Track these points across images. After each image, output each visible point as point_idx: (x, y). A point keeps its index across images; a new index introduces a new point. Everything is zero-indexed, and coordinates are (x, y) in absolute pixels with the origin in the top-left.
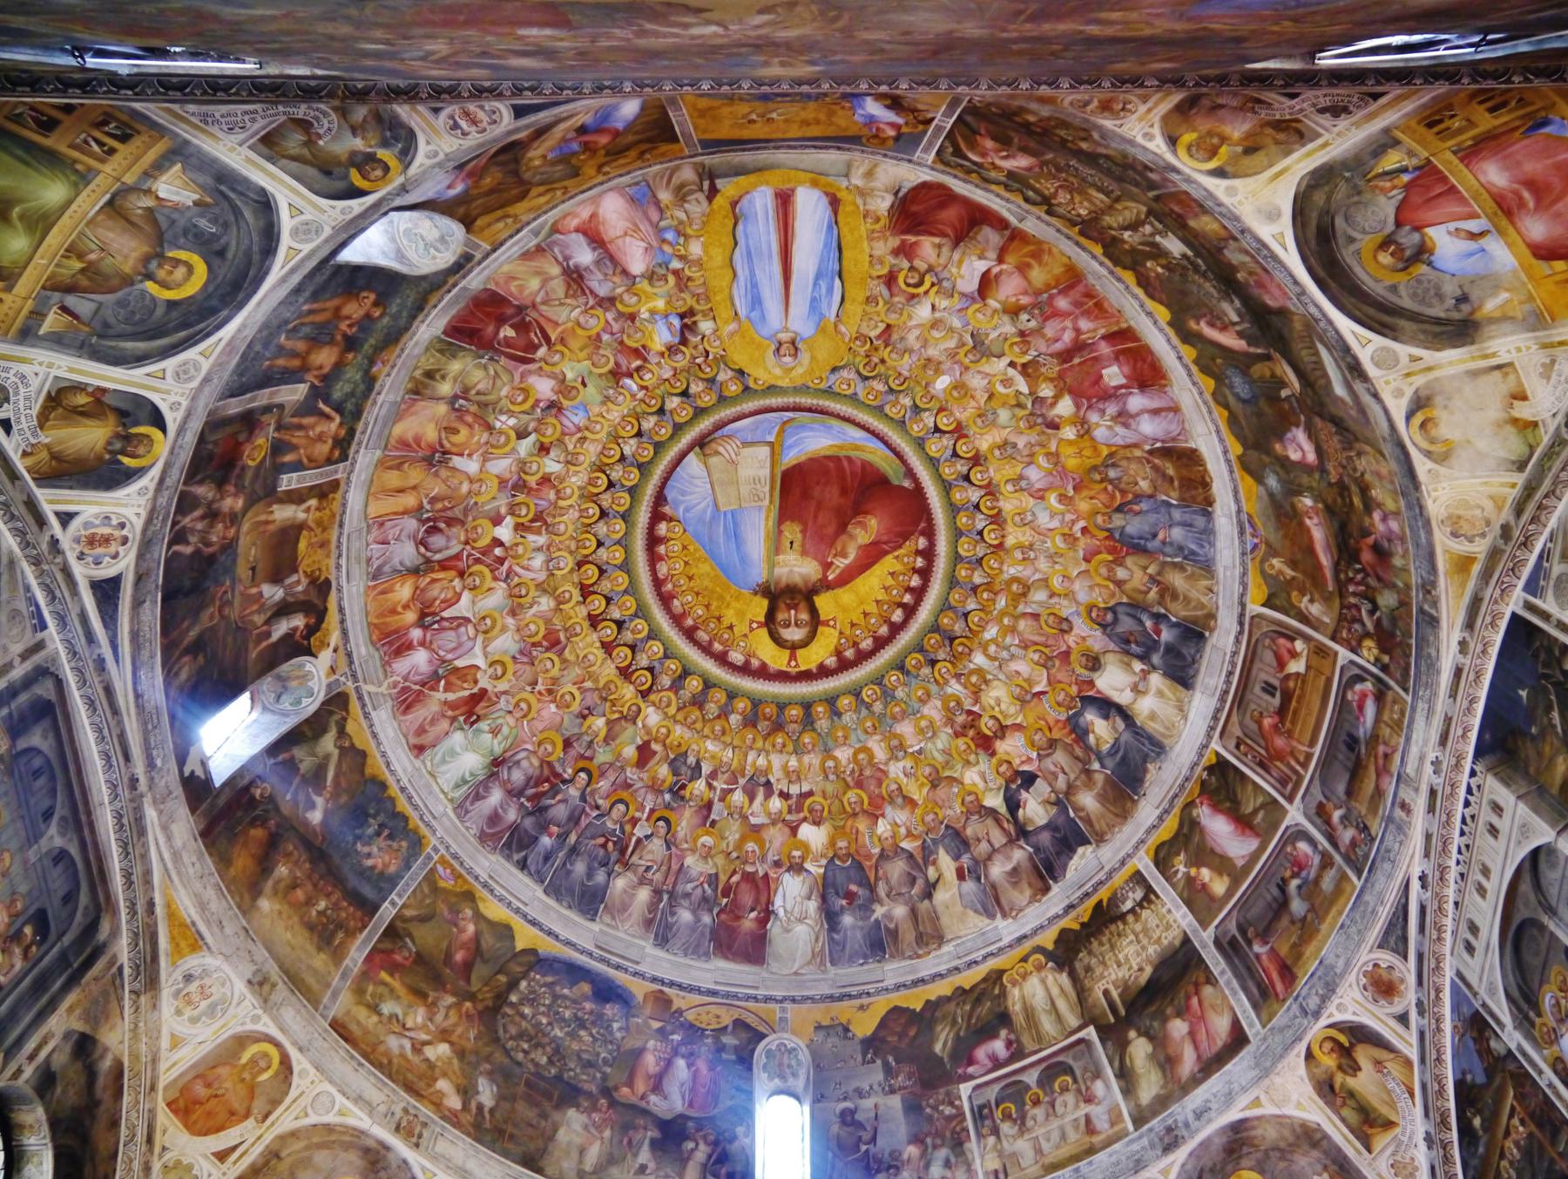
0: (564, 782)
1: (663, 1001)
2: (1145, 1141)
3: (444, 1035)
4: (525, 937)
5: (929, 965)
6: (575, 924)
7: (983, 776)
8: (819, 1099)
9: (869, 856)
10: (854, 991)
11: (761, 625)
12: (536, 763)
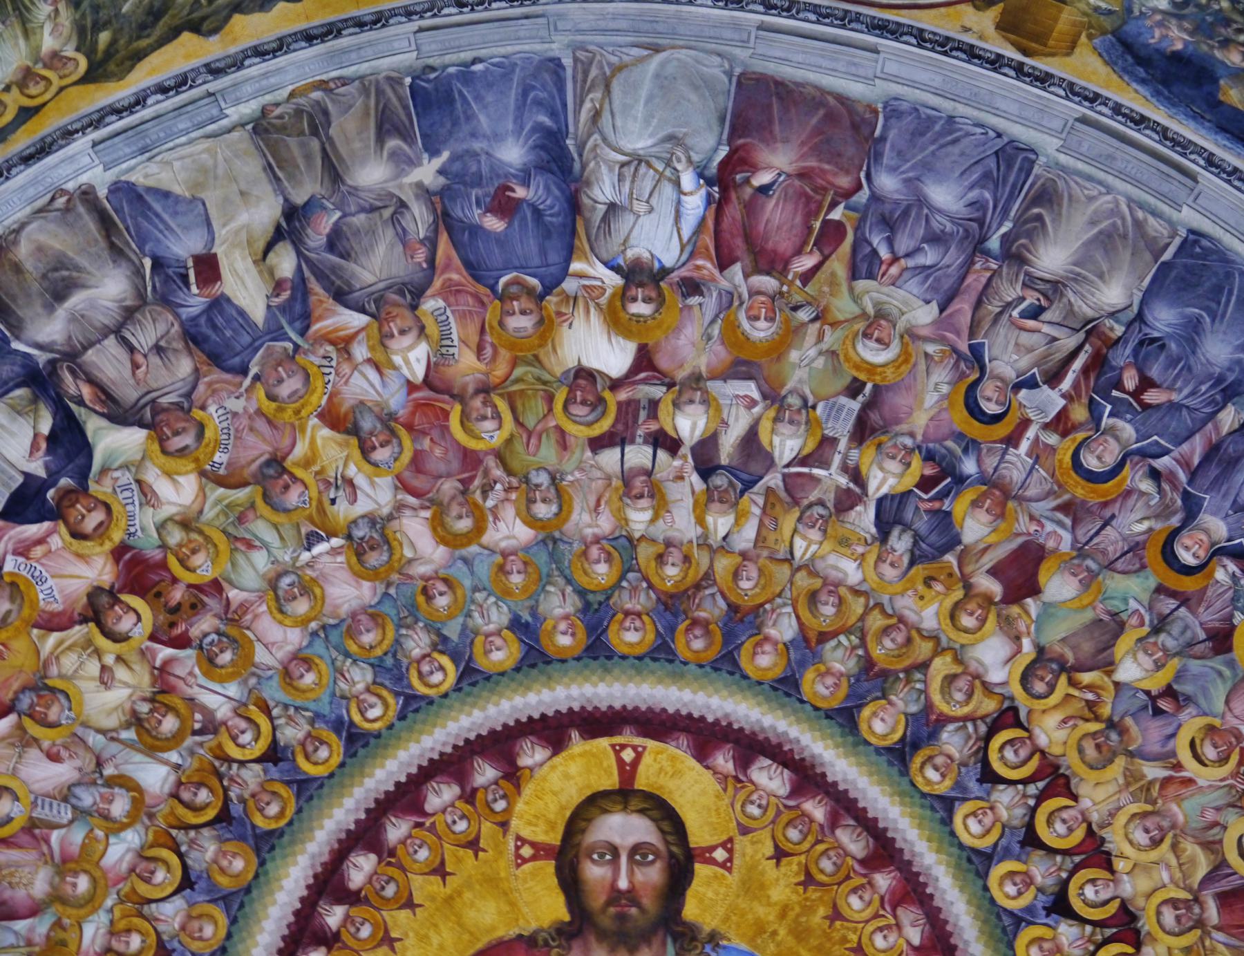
5: (301, 67)
7: (147, 494)
9: (451, 292)
11: (705, 855)
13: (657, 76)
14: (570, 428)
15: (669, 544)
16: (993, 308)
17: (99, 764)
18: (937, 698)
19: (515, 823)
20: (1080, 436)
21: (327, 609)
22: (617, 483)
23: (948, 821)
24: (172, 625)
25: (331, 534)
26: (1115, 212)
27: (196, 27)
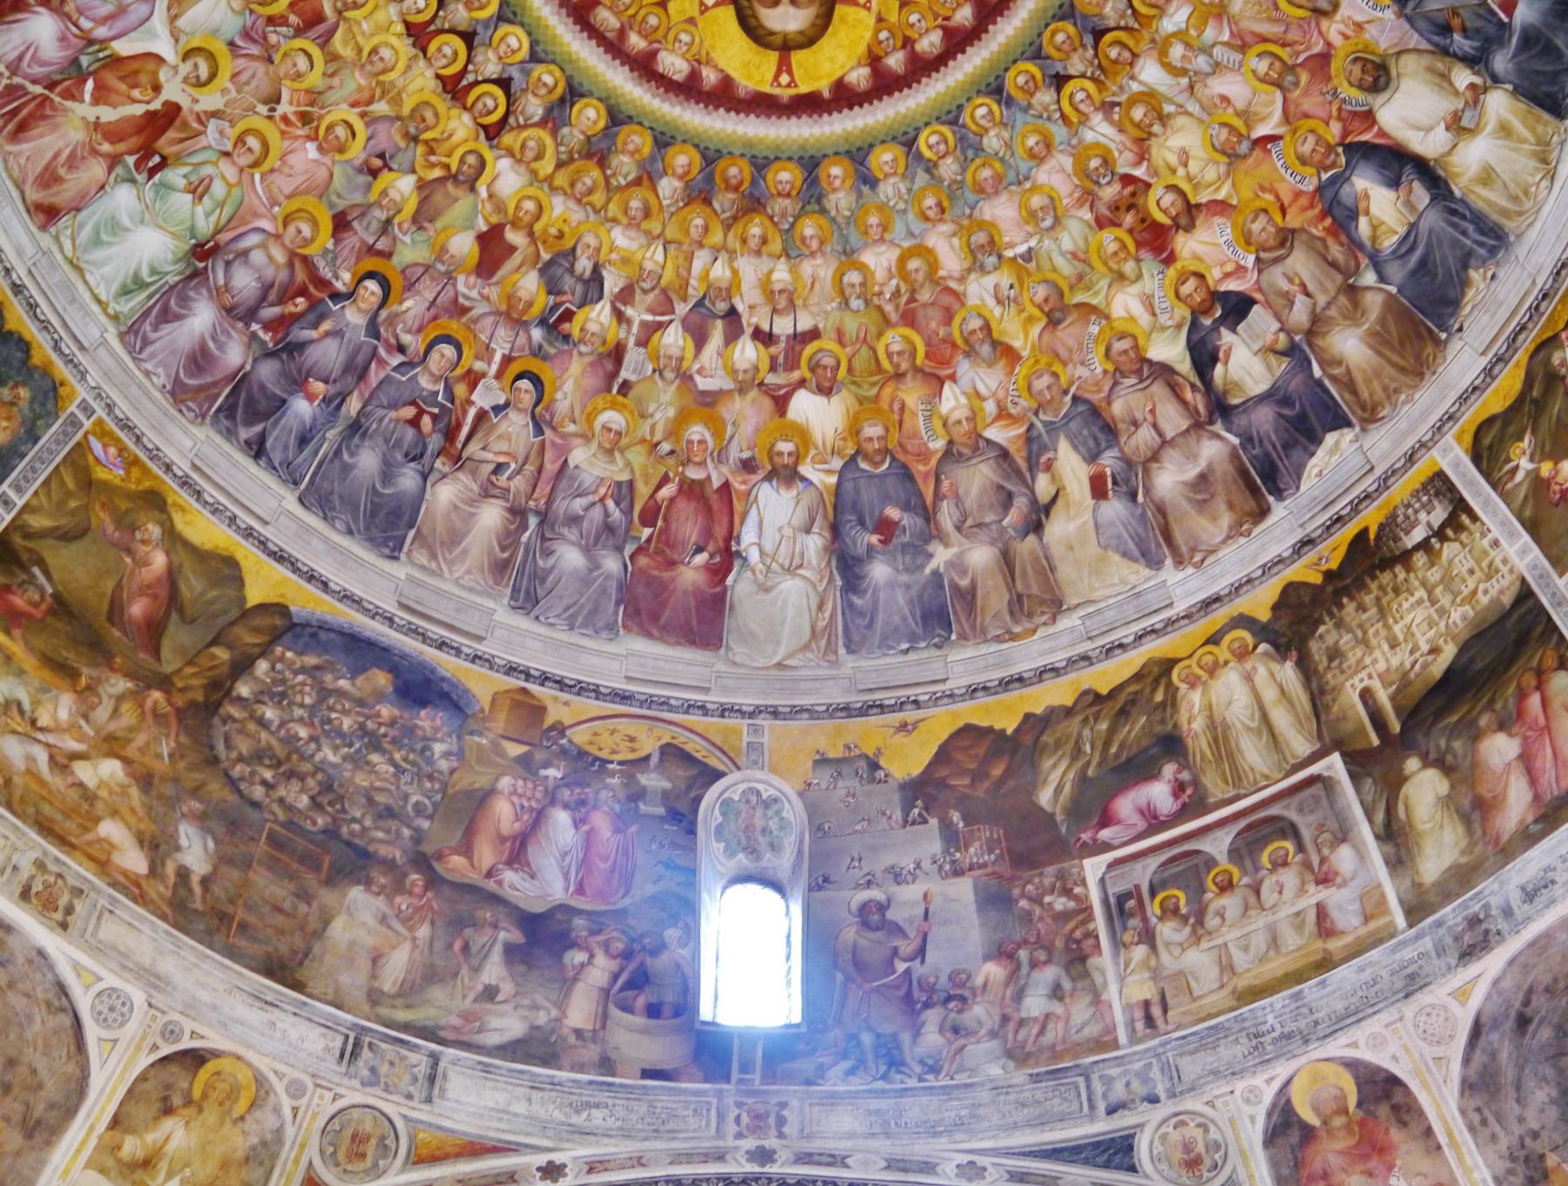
0: (336, 296)
1: (528, 710)
2: (1427, 944)
3: (111, 745)
4: (263, 583)
5: (1028, 654)
6: (361, 563)
8: (820, 883)
9: (924, 455)
10: (888, 697)
12: (280, 256)
13: (778, 643)
14: (834, 347)
15: (758, 253)
16: (530, 468)
17: (1191, 87)
18: (549, 141)
19: (872, 21)
20: (458, 371)
21: (1017, 198)
22: (799, 302)
23: (534, 44)
24: (1133, 194)
25: (1014, 259)
26: (451, 563)
27: (1098, 698)
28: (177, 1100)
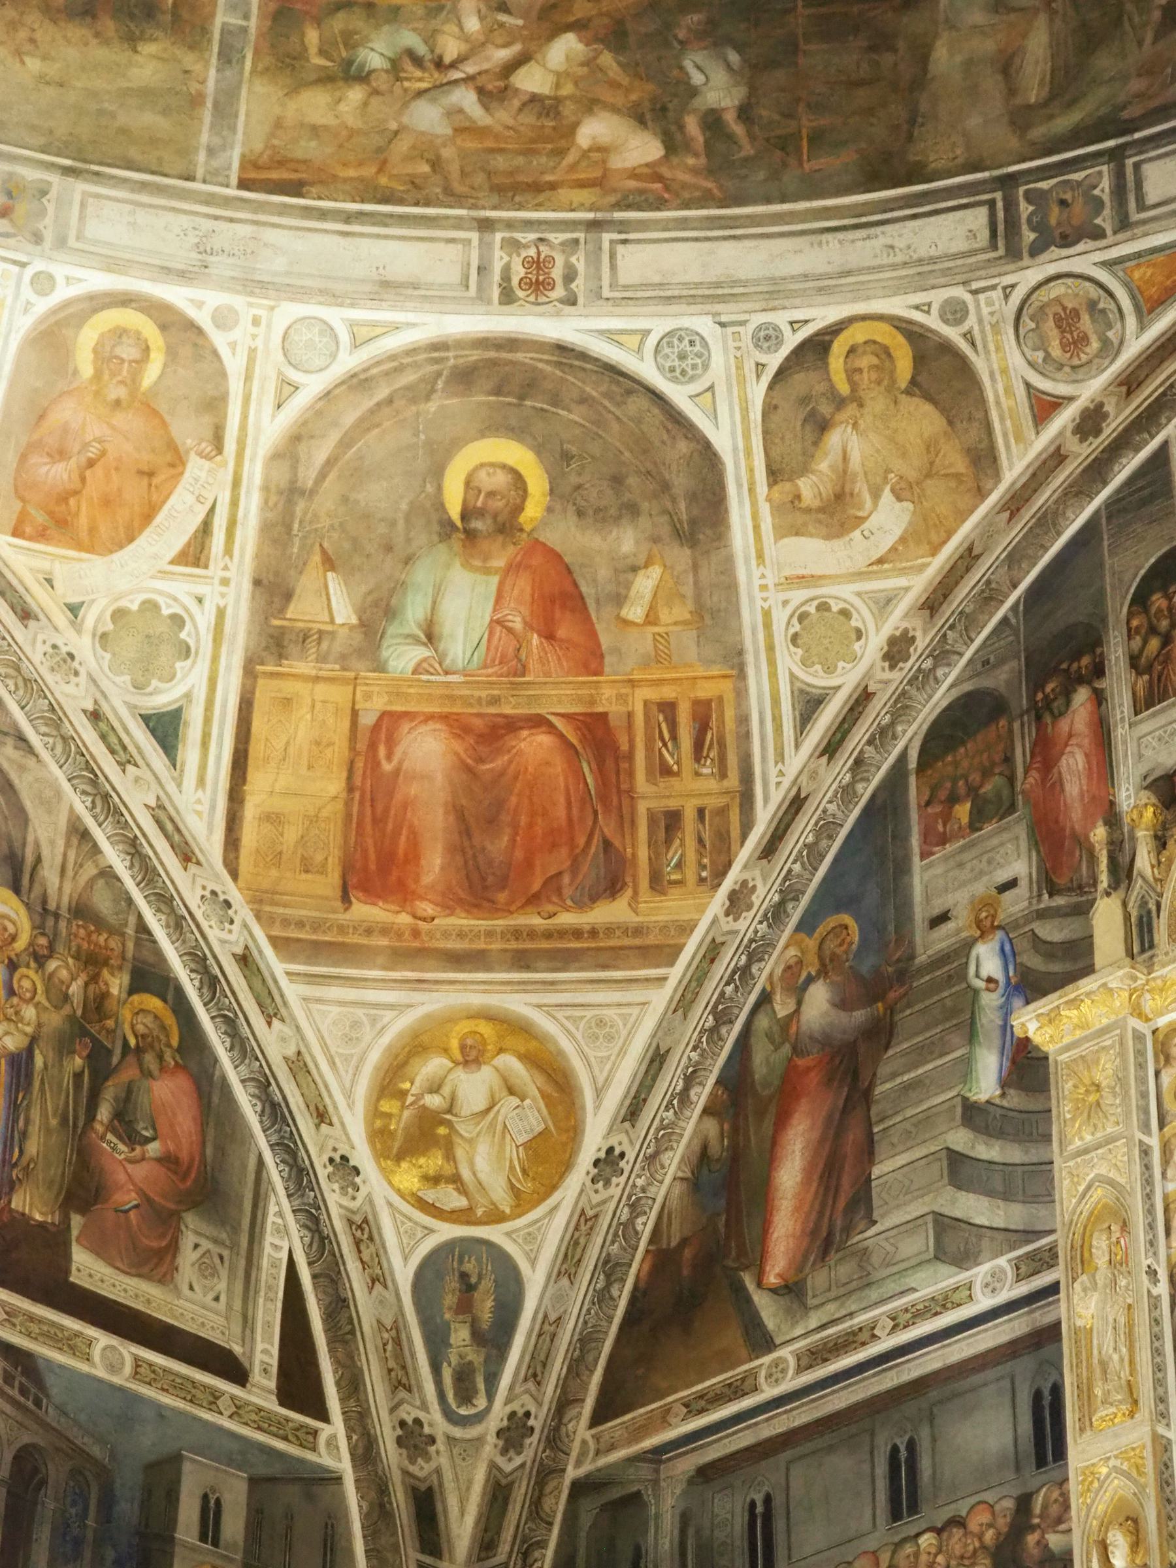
28: (825, 409)
